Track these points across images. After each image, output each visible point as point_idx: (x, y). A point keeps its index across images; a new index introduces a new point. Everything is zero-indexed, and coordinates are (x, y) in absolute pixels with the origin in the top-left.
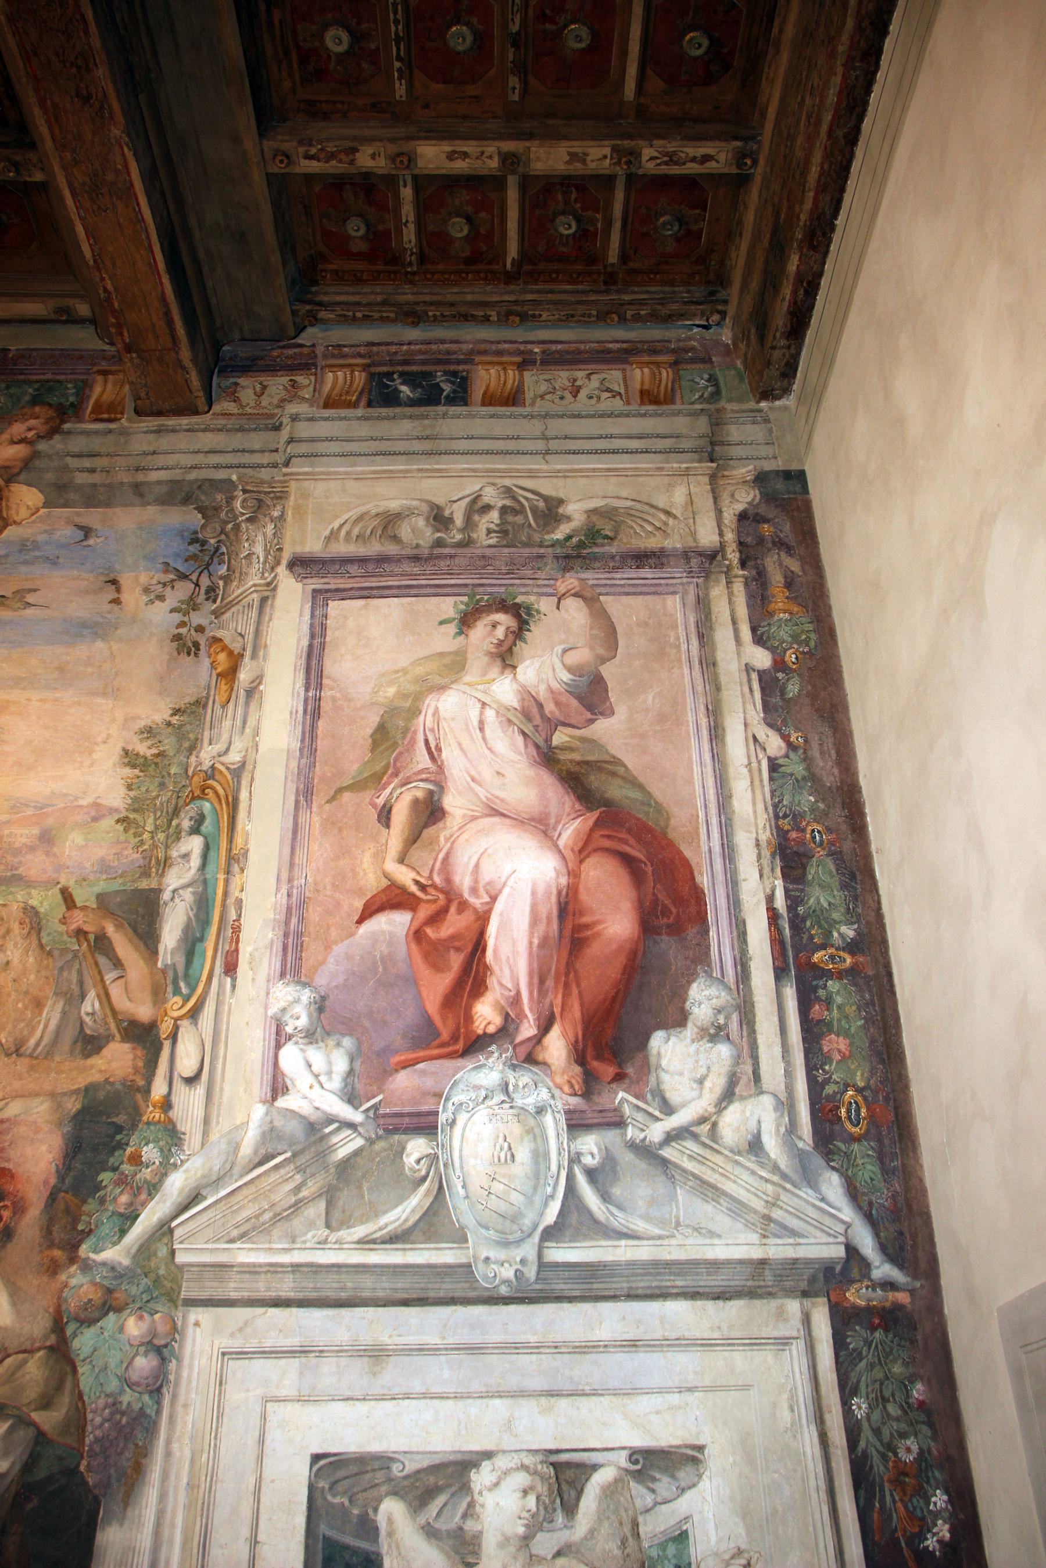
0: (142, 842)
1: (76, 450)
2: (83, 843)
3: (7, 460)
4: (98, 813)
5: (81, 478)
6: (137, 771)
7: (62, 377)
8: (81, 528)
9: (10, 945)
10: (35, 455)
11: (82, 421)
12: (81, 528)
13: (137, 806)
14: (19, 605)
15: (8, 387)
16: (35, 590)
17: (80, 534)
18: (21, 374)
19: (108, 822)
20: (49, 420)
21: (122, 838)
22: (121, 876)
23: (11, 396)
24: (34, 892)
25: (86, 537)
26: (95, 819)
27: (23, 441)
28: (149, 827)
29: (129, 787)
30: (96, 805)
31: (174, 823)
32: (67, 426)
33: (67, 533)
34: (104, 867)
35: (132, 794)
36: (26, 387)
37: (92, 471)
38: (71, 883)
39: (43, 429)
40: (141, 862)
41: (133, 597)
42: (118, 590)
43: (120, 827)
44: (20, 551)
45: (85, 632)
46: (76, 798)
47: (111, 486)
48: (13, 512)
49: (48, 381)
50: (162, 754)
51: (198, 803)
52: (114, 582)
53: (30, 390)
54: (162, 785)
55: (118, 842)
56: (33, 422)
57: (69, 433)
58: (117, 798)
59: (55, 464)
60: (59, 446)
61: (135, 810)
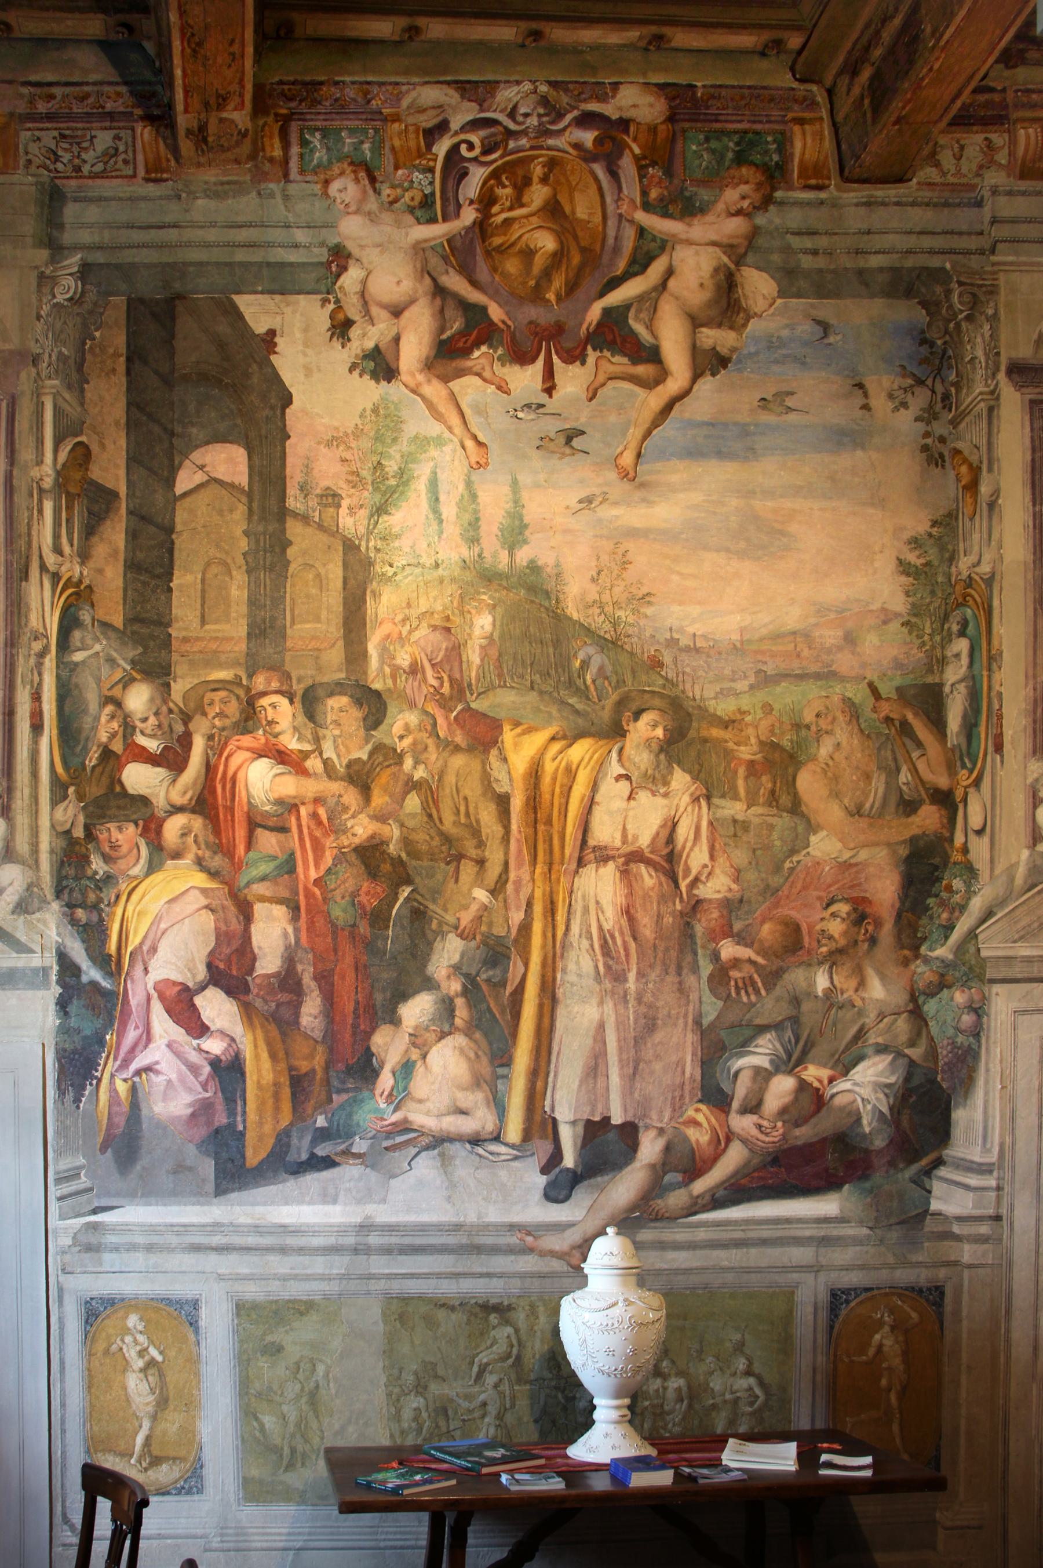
0: (924, 644)
1: (793, 225)
2: (878, 643)
3: (731, 237)
4: (886, 617)
5: (807, 262)
6: (911, 579)
7: (758, 127)
8: (818, 322)
9: (838, 731)
10: (755, 232)
11: (791, 188)
12: (818, 322)
13: (916, 610)
14: (780, 409)
15: (707, 140)
16: (792, 393)
17: (819, 331)
18: (717, 121)
19: (895, 626)
20: (759, 186)
21: (908, 640)
22: (912, 672)
23: (713, 151)
24: (848, 686)
25: (826, 335)
26: (885, 623)
27: (739, 212)
28: (928, 630)
29: (907, 594)
30: (884, 610)
31: (946, 627)
32: (778, 194)
33: (806, 329)
34: (898, 665)
35: (910, 600)
36: (725, 139)
37: (815, 253)
38: (875, 679)
39: (757, 197)
40: (925, 661)
41: (879, 402)
42: (866, 395)
43: (905, 630)
44: (769, 348)
45: (846, 440)
46: (868, 603)
47: (834, 272)
48: (751, 302)
49: (746, 132)
50: (928, 564)
51: (962, 609)
52: (860, 386)
53: (731, 145)
54: (933, 593)
55: (905, 643)
56: (744, 188)
57: (782, 203)
58: (899, 604)
59: (777, 243)
60: (777, 221)
61: (915, 615)
